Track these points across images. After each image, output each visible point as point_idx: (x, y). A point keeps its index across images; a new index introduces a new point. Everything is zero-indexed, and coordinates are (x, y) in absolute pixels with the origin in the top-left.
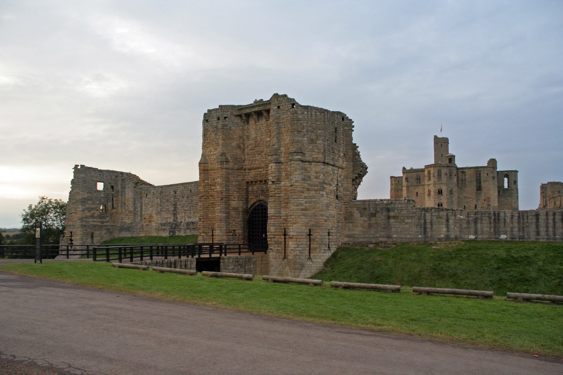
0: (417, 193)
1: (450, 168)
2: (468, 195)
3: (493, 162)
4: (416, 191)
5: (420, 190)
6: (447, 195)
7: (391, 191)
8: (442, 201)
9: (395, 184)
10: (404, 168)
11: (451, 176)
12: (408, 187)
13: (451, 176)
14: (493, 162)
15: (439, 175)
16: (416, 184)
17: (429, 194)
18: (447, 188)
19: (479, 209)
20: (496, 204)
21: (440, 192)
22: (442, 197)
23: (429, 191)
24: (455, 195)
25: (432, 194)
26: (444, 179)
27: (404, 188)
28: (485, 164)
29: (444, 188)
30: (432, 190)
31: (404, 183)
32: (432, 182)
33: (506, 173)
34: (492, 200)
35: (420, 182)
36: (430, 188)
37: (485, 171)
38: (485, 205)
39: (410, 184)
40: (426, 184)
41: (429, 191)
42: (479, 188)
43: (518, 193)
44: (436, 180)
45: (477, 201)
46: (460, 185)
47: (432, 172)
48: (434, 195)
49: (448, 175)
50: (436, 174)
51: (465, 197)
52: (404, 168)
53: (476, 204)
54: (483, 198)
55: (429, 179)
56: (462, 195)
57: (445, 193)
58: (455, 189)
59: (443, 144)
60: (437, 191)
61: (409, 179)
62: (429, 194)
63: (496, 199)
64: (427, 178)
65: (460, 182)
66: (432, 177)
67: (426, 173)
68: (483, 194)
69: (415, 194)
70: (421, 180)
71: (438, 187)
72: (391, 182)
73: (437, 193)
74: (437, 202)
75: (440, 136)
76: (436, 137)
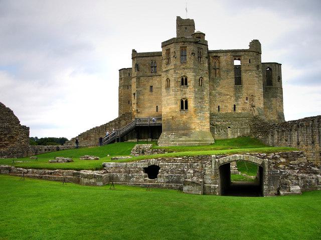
0: (151, 87)
1: (200, 46)
2: (223, 91)
3: (256, 46)
4: (150, 84)
5: (155, 82)
6: (194, 87)
7: (120, 88)
8: (187, 96)
9: (125, 78)
10: (134, 51)
11: (200, 57)
12: (138, 78)
13: (200, 57)
14: (256, 46)
15: (183, 55)
16: (150, 74)
17: (168, 87)
18: (195, 76)
19: (239, 111)
20: (262, 106)
21: (184, 82)
22: (188, 90)
23: (168, 80)
24: (207, 86)
25: (172, 84)
26: (190, 61)
27: (134, 80)
28: (248, 48)
29: (190, 76)
30: (172, 79)
31: (134, 73)
32: (171, 66)
33: (268, 65)
34: (256, 98)
35: (156, 72)
36: (169, 76)
37: (246, 57)
38: (248, 106)
39: (141, 74)
40: (164, 70)
41: (168, 80)
42: (238, 81)
43: (282, 94)
44: (178, 63)
45: (236, 100)
46: (213, 75)
47: (172, 50)
48: (176, 87)
49: (196, 56)
50: (178, 54)
51: (220, 94)
52: (134, 51)
53: (235, 103)
54: (245, 95)
55: (168, 63)
56: (214, 90)
57: (191, 83)
58: (206, 79)
59: (188, 27)
60: (180, 80)
61: (141, 67)
62: (168, 87)
63: (262, 98)
64: (164, 62)
65: (213, 71)
66: (172, 59)
67: (164, 54)
68: (244, 91)
69: (149, 88)
70: (158, 69)
71: (181, 73)
72: (120, 76)
73: (180, 83)
74: (180, 97)
75: (184, 17)
76: (179, 19)
